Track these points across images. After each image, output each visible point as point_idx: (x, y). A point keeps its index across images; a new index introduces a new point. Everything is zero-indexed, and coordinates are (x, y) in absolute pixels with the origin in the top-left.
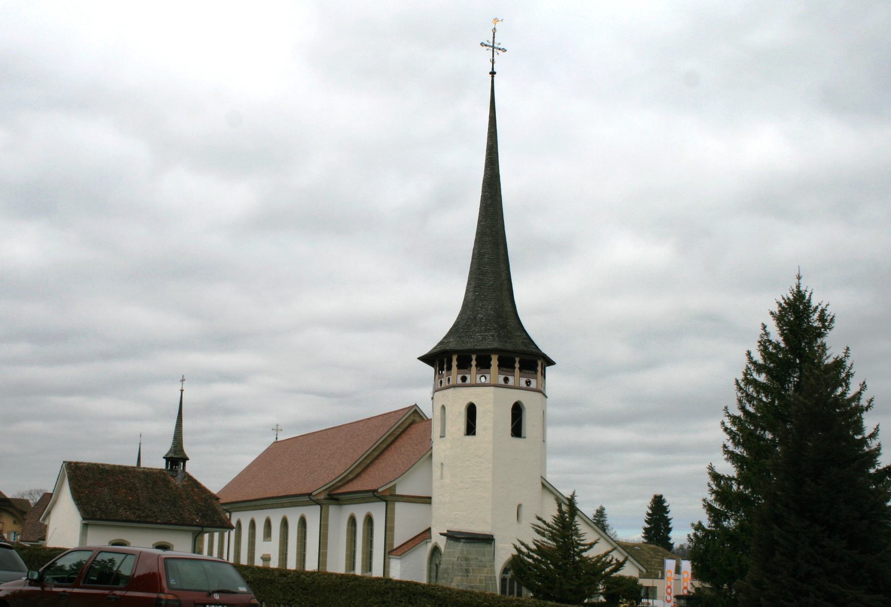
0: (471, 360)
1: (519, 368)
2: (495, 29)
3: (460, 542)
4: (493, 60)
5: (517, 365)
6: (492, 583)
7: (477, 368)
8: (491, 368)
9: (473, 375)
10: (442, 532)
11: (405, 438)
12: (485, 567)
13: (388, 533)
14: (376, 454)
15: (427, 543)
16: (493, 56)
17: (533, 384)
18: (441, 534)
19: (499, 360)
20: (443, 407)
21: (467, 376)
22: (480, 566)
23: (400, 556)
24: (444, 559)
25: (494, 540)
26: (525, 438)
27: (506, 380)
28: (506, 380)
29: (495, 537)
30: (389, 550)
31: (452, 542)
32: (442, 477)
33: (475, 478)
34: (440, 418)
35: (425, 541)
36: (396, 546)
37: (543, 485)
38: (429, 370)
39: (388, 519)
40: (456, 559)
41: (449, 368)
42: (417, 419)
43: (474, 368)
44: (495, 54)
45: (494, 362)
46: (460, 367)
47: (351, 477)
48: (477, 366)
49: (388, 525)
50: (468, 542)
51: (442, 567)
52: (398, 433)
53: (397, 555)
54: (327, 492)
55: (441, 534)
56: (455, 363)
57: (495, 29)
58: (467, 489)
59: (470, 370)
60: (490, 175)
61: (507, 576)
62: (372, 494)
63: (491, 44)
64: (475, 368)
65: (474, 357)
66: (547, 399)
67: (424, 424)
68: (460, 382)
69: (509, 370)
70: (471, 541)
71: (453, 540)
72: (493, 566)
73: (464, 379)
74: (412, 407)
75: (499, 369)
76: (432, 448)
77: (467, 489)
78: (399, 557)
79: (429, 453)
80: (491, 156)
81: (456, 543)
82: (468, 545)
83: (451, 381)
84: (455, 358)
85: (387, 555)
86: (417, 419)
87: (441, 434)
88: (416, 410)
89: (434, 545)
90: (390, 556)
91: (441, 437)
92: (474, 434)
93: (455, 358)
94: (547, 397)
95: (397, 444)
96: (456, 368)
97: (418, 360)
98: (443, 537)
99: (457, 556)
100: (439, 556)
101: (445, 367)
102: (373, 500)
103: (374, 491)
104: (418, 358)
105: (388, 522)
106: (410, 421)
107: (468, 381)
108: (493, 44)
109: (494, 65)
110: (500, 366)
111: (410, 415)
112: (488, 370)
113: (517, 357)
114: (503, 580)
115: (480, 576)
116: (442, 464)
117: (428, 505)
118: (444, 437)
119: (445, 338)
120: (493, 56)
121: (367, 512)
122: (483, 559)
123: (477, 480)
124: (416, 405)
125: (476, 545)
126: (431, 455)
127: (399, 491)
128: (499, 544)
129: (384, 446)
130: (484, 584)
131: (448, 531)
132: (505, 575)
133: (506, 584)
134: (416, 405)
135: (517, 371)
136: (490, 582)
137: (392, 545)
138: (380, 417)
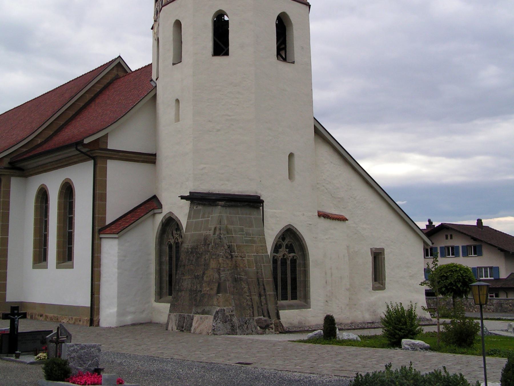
3: (218, 205)
6: (264, 266)
13: (97, 202)
14: (71, 113)
15: (154, 214)
18: (183, 197)
22: (247, 241)
23: (118, 234)
25: (262, 202)
26: (293, 63)
30: (100, 228)
31: (200, 207)
32: (177, 119)
33: (230, 116)
35: (151, 213)
36: (108, 223)
39: (97, 183)
40: (211, 232)
42: (121, 74)
47: (39, 141)
49: (97, 192)
50: (229, 206)
52: (98, 90)
53: (114, 233)
54: (7, 160)
55: (183, 197)
58: (218, 130)
61: (278, 255)
70: (233, 203)
71: (204, 205)
72: (264, 241)
74: (116, 59)
76: (156, 86)
77: (218, 130)
78: (116, 236)
79: (152, 94)
81: (209, 209)
82: (228, 210)
85: (97, 234)
86: (121, 74)
87: (173, 60)
88: (119, 62)
89: (167, 217)
90: (102, 236)
91: (174, 64)
92: (227, 54)
98: (184, 201)
99: (213, 227)
100: (175, 232)
102: (75, 160)
105: (97, 188)
114: (275, 261)
116: (177, 101)
121: (64, 179)
124: (120, 57)
125: (239, 210)
126: (155, 96)
127: (113, 144)
128: (268, 209)
129: (82, 104)
130: (255, 268)
134: (120, 57)
136: (262, 265)
137: (104, 219)
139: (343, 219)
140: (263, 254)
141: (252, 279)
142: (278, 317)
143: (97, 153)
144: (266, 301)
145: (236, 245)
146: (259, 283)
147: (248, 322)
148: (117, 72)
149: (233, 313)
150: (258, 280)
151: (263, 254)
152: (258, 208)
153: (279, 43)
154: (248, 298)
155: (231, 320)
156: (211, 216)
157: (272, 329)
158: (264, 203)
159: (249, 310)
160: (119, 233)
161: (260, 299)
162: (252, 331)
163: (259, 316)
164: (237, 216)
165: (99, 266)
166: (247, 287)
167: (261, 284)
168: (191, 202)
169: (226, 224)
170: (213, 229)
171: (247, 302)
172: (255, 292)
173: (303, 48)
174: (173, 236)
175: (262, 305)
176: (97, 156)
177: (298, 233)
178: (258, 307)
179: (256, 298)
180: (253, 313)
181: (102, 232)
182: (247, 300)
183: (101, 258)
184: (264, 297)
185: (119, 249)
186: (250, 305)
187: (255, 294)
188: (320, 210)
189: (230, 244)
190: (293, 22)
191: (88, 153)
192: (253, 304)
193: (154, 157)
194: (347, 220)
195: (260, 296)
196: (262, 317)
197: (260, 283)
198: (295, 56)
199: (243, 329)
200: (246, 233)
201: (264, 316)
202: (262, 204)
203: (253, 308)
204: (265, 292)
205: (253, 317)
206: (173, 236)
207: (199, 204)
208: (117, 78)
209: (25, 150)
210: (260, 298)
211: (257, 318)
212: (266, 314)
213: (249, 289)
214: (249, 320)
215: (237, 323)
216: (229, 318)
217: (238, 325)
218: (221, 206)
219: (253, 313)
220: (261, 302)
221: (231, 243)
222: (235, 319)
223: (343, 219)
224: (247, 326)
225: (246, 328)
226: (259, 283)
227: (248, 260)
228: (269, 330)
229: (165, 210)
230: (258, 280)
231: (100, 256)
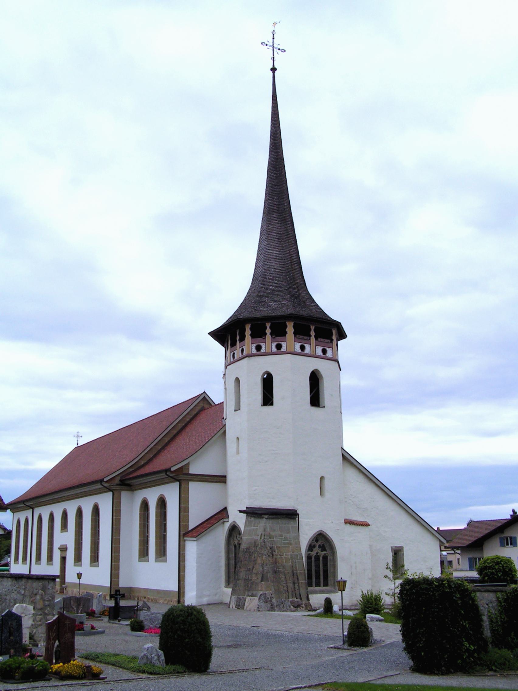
0: (266, 328)
1: (315, 336)
2: (274, 31)
3: (263, 518)
4: (274, 58)
5: (313, 333)
6: (298, 562)
7: (272, 337)
8: (287, 335)
9: (268, 344)
10: (241, 509)
11: (196, 423)
12: (291, 544)
13: (182, 514)
14: (167, 439)
15: (224, 522)
16: (273, 55)
17: (329, 353)
18: (241, 511)
19: (294, 327)
20: (237, 380)
21: (262, 344)
22: (285, 544)
23: (196, 537)
24: (244, 538)
25: (298, 514)
26: (324, 407)
27: (303, 348)
28: (303, 348)
29: (298, 512)
30: (184, 532)
31: (252, 519)
32: (238, 452)
33: (274, 451)
34: (234, 391)
35: (222, 521)
36: (190, 528)
37: (344, 457)
38: (218, 349)
40: (259, 537)
41: (242, 339)
42: (206, 406)
43: (268, 336)
44: (275, 53)
45: (290, 329)
46: (253, 336)
47: (142, 463)
48: (271, 334)
49: (182, 506)
51: (243, 546)
52: (188, 420)
54: (119, 478)
55: (241, 511)
56: (248, 333)
57: (274, 31)
58: (266, 462)
59: (265, 338)
60: (275, 158)
61: (312, 553)
62: (164, 474)
63: (272, 44)
64: (270, 336)
65: (268, 325)
66: (341, 371)
67: (213, 408)
68: (254, 351)
69: (305, 338)
70: (275, 516)
73: (259, 348)
74: (201, 394)
75: (295, 336)
76: (225, 425)
77: (266, 462)
80: (275, 141)
81: (258, 520)
82: (271, 521)
83: (244, 351)
84: (248, 328)
85: (182, 538)
86: (206, 406)
87: (235, 408)
89: (232, 525)
90: (185, 538)
91: (235, 411)
92: (272, 404)
93: (248, 328)
94: (340, 370)
95: (187, 430)
96: (250, 337)
97: (209, 335)
98: (242, 514)
100: (238, 536)
101: (238, 338)
103: (167, 470)
104: (209, 334)
105: (182, 503)
106: (199, 408)
107: (263, 350)
108: (273, 44)
109: (275, 62)
110: (295, 333)
111: (200, 402)
112: (285, 337)
113: (313, 325)
114: (309, 558)
115: (286, 555)
116: (238, 438)
117: (223, 484)
118: (240, 410)
119: (264, 210)
120: (273, 55)
121: (159, 495)
122: (288, 535)
123: (277, 452)
124: (204, 392)
125: (280, 521)
126: (225, 432)
127: (194, 470)
128: (303, 519)
130: (290, 563)
131: (247, 508)
132: (309, 552)
133: (311, 562)
134: (204, 392)
135: (313, 339)
137: (187, 526)
138: (169, 409)
139: (367, 525)
140: (297, 553)
142: (308, 599)
143: (181, 477)
144: (299, 587)
145: (277, 547)
148: (202, 405)
151: (297, 553)
152: (295, 519)
153: (312, 394)
154: (284, 585)
155: (271, 601)
156: (259, 525)
157: (303, 608)
158: (299, 515)
160: (197, 536)
163: (293, 598)
164: (278, 525)
165: (184, 561)
167: (295, 574)
168: (247, 516)
169: (269, 531)
170: (260, 535)
173: (332, 395)
174: (237, 538)
175: (295, 591)
176: (181, 480)
177: (327, 536)
178: (292, 592)
179: (291, 585)
180: (288, 596)
181: (186, 536)
183: (186, 555)
185: (197, 548)
186: (286, 590)
188: (347, 518)
189: (272, 546)
190: (323, 376)
191: (175, 477)
193: (224, 478)
194: (369, 525)
195: (294, 583)
196: (295, 599)
198: (325, 402)
200: (284, 538)
201: (297, 598)
202: (297, 516)
206: (237, 538)
207: (252, 516)
208: (203, 409)
209: (131, 470)
210: (294, 586)
212: (298, 596)
216: (269, 599)
217: (276, 604)
218: (266, 518)
219: (288, 596)
220: (294, 588)
221: (272, 545)
222: (274, 600)
223: (367, 525)
225: (282, 606)
227: (285, 557)
228: (300, 608)
229: (231, 519)
231: (185, 554)
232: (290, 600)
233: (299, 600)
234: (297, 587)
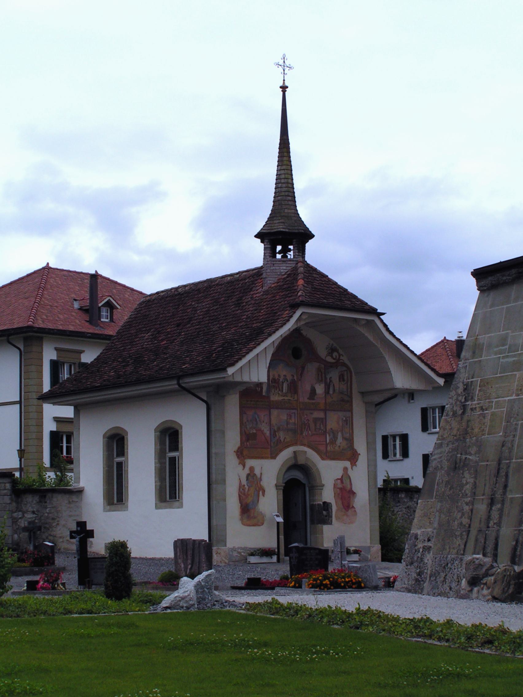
141: (488, 461)
144: (500, 517)
146: (498, 472)
147: (449, 565)
149: (429, 544)
150: (499, 464)
154: (467, 508)
159: (459, 538)
161: (489, 512)
162: (451, 589)
163: (474, 553)
166: (472, 480)
171: (461, 517)
172: (483, 495)
175: (488, 527)
178: (480, 531)
179: (482, 508)
180: (465, 546)
182: (463, 514)
184: (499, 506)
186: (465, 525)
187: (483, 499)
192: (472, 525)
195: (492, 502)
196: (480, 556)
197: (501, 471)
199: (437, 582)
201: (484, 555)
203: (468, 532)
204: (504, 493)
205: (463, 555)
210: (491, 509)
211: (470, 558)
212: (489, 549)
213: (475, 485)
214: (453, 560)
215: (429, 566)
217: (429, 572)
219: (465, 546)
220: (489, 518)
222: (429, 558)
224: (446, 575)
225: (442, 579)
226: (498, 472)
227: (493, 414)
230: (499, 464)
232: (468, 558)
233: (488, 560)
234: (495, 514)
